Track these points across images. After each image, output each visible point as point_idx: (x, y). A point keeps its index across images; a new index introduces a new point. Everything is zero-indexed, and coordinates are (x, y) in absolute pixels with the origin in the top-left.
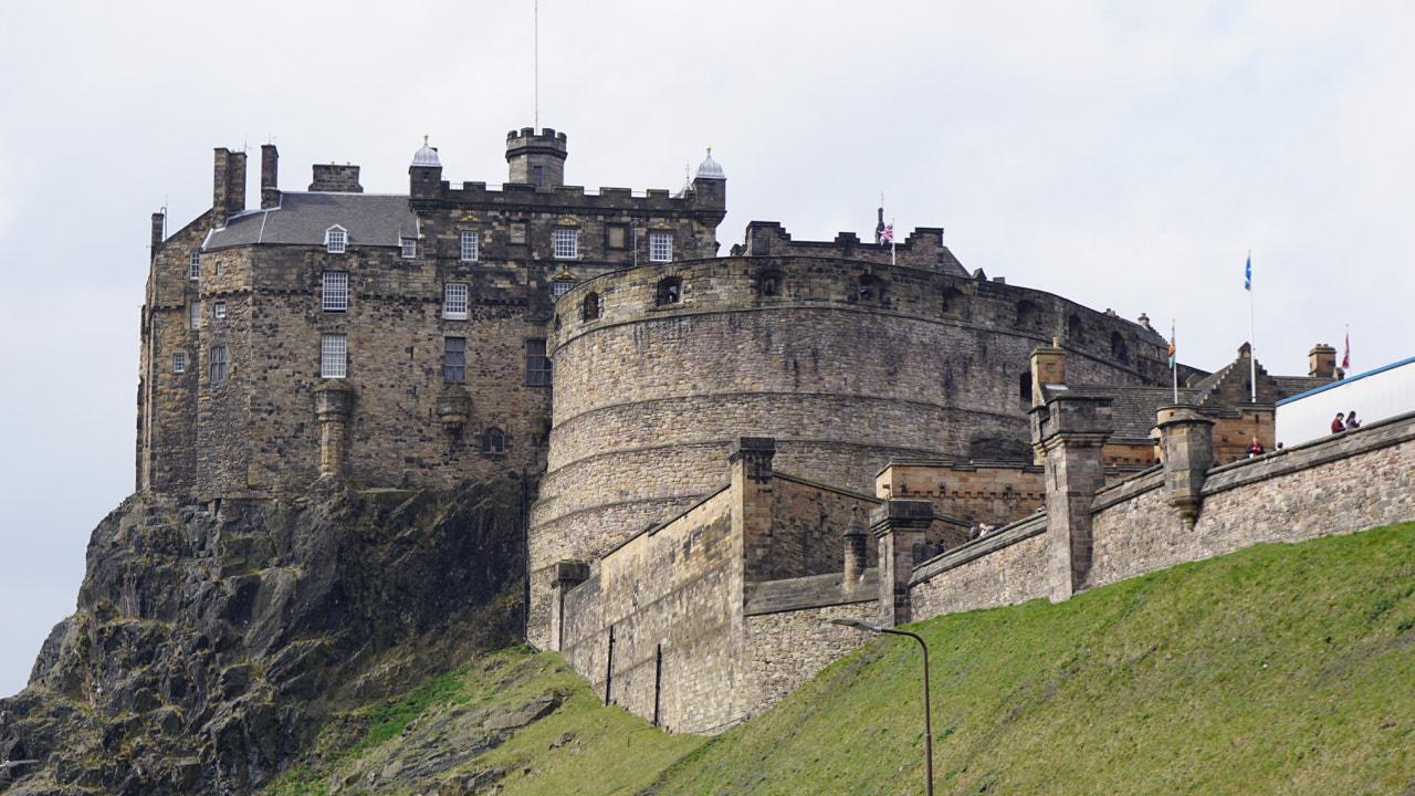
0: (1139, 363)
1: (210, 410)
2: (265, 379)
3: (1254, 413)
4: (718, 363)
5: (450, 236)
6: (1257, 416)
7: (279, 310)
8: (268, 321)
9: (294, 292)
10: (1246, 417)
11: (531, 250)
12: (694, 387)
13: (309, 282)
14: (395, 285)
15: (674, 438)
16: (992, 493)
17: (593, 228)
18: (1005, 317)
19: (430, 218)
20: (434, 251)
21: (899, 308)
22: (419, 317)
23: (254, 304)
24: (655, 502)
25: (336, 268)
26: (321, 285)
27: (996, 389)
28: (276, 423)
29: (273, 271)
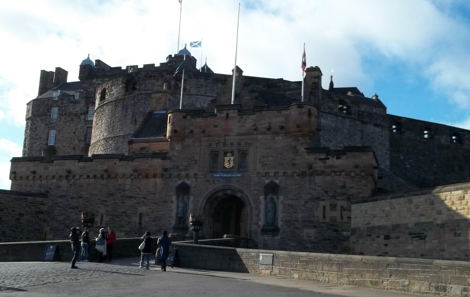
0: (359, 115)
2: (32, 147)
3: (225, 112)
5: (92, 89)
8: (35, 126)
9: (42, 115)
10: (219, 115)
13: (46, 111)
14: (71, 109)
16: (60, 176)
20: (85, 95)
21: (191, 91)
22: (79, 120)
25: (55, 105)
26: (51, 112)
29: (37, 108)
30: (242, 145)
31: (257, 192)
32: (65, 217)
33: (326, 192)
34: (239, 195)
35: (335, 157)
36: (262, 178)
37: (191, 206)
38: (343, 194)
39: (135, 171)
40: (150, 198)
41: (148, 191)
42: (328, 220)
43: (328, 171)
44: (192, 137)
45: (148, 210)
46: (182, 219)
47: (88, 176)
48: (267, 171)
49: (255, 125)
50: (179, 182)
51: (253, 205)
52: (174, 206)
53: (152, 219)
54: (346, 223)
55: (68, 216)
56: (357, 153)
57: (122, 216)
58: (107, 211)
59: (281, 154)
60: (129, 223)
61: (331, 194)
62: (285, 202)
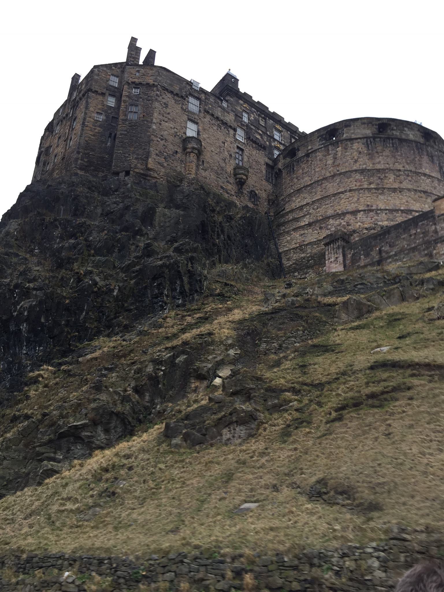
1: (126, 131)
2: (160, 124)
4: (414, 159)
5: (238, 108)
7: (168, 98)
8: (164, 101)
9: (177, 95)
11: (267, 131)
12: (404, 167)
15: (396, 185)
17: (287, 134)
19: (232, 97)
23: (158, 90)
24: (391, 211)
25: (196, 95)
28: (164, 145)
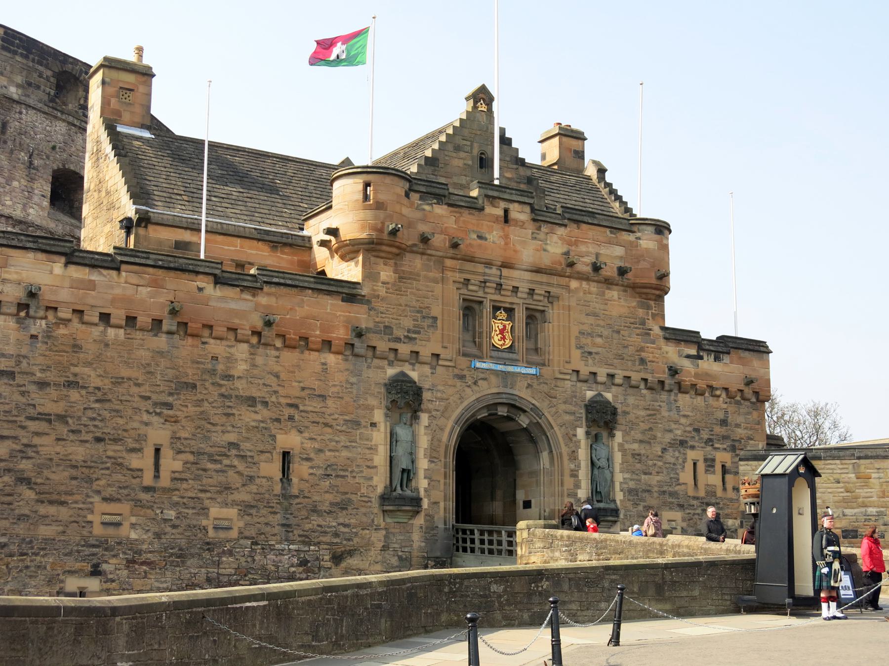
3: (503, 205)
6: (506, 211)
10: (489, 210)
18: (38, 87)
27: (15, 184)
30: (535, 297)
31: (572, 418)
32: (18, 447)
33: (697, 430)
34: (524, 421)
35: (713, 356)
36: (579, 384)
37: (424, 442)
38: (725, 438)
39: (268, 324)
40: (310, 409)
41: (303, 389)
42: (702, 493)
43: (702, 385)
44: (423, 254)
45: (308, 445)
46: (408, 474)
47: (105, 318)
48: (594, 370)
49: (567, 253)
50: (391, 372)
51: (565, 450)
52: (380, 437)
53: (320, 472)
54: (731, 500)
55: (26, 446)
56: (747, 354)
57: (228, 456)
58: (175, 438)
59: (618, 332)
60: (251, 478)
61: (705, 435)
62: (627, 446)
